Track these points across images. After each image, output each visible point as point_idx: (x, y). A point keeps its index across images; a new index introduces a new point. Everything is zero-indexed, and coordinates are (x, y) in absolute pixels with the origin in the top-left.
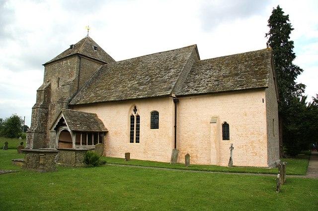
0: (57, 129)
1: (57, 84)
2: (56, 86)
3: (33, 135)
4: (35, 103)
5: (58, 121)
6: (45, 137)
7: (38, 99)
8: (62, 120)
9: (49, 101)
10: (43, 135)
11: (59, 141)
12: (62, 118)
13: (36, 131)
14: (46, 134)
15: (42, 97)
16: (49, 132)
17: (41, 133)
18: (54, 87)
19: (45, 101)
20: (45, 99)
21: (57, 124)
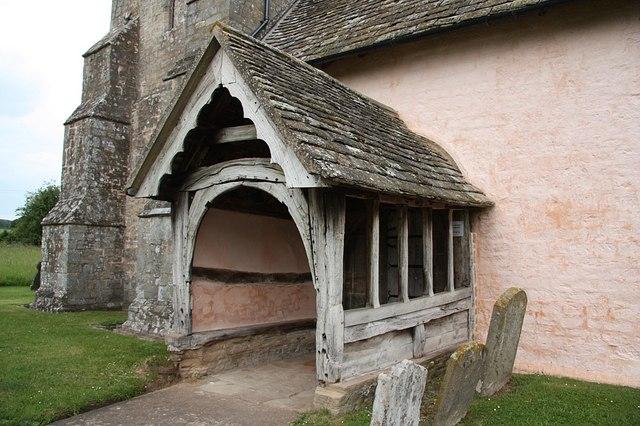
0: (174, 191)
1: (164, 17)
2: (163, 24)
3: (65, 236)
4: (78, 102)
5: (189, 121)
6: (119, 243)
7: (90, 87)
8: (224, 109)
9: (132, 91)
10: (109, 236)
11: (196, 273)
12: (221, 93)
13: (78, 220)
14: (122, 228)
15: (105, 76)
16: (131, 219)
17: (102, 224)
18: (153, 30)
19: (114, 92)
20: (113, 82)
21: (176, 146)
